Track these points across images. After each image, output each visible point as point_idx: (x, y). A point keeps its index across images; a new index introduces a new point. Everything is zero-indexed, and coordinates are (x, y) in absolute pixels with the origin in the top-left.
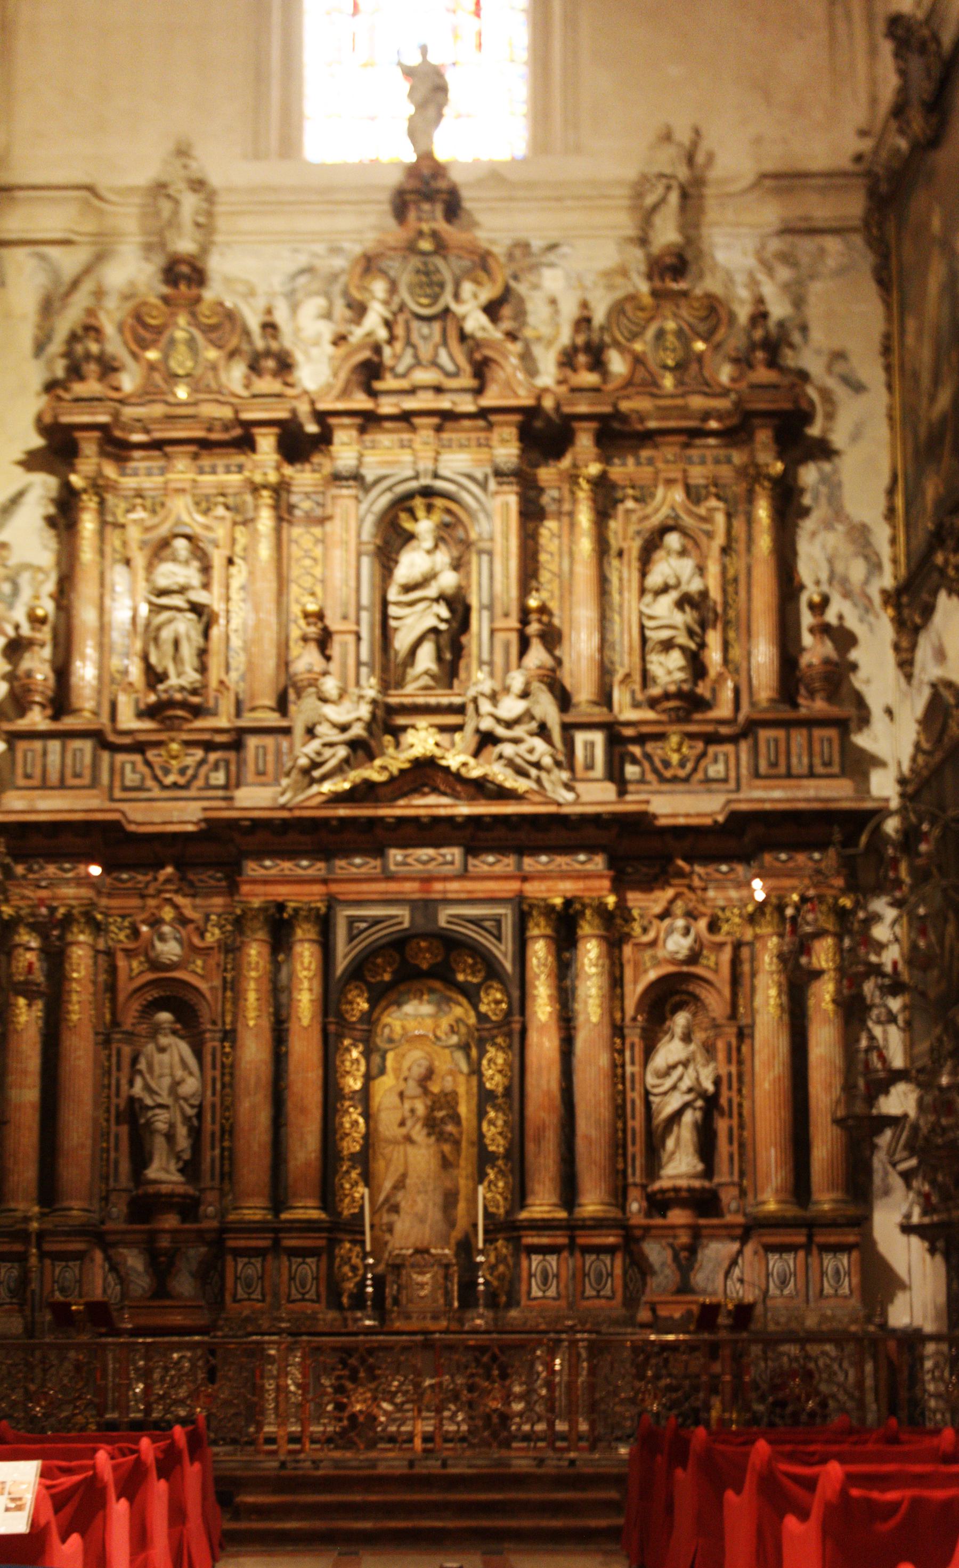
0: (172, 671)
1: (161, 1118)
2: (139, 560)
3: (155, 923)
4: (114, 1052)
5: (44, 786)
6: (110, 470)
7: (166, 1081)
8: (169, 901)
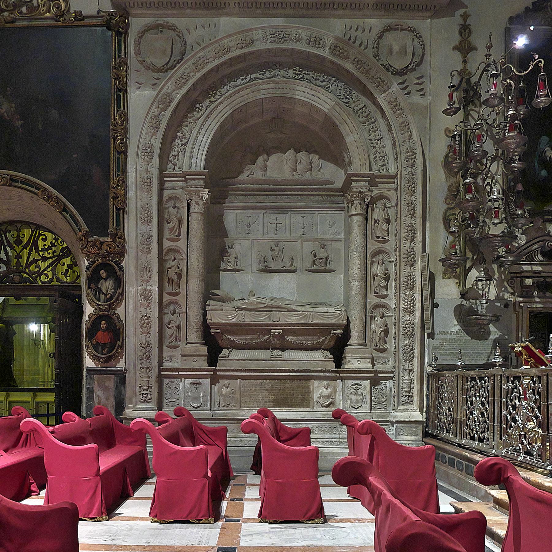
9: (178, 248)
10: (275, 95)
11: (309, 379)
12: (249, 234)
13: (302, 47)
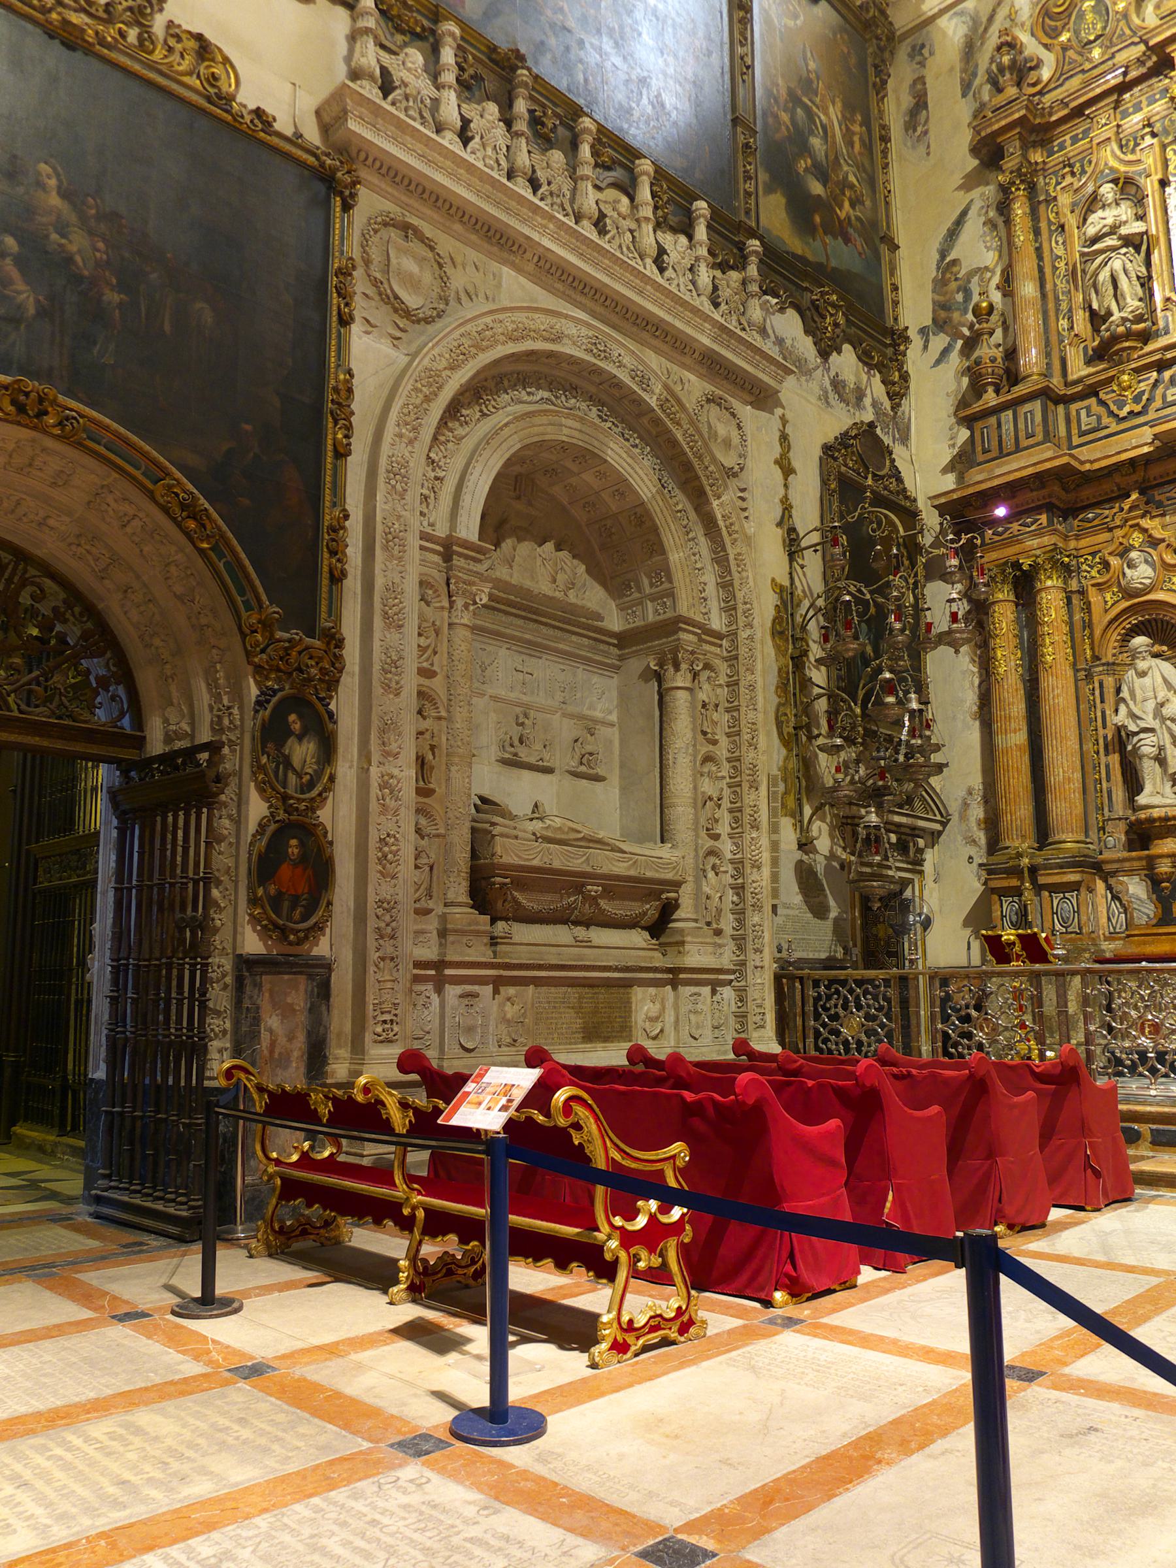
0: (1114, 307)
1: (1147, 742)
2: (1071, 221)
3: (1123, 553)
4: (1097, 685)
5: (1002, 454)
6: (1037, 156)
7: (1151, 705)
8: (1138, 525)
9: (432, 693)
10: (580, 443)
11: (628, 984)
12: (483, 683)
13: (623, 376)
